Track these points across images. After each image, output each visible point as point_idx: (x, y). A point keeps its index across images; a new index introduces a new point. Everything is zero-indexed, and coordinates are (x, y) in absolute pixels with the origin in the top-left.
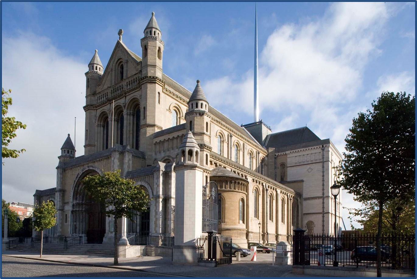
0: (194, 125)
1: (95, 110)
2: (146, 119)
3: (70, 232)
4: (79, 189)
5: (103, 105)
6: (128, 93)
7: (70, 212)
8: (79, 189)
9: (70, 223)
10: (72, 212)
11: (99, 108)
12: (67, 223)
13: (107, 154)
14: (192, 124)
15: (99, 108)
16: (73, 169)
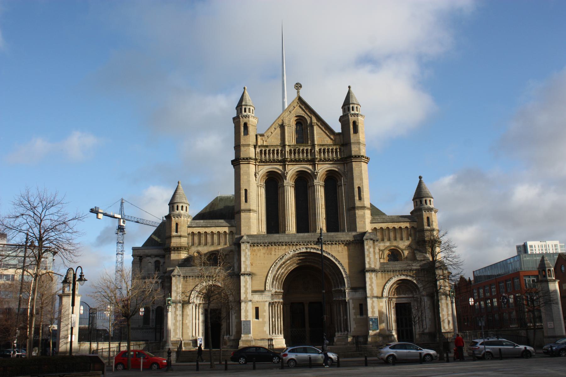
0: (432, 222)
1: (257, 166)
2: (364, 201)
3: (268, 332)
4: (278, 274)
5: (273, 163)
6: (322, 162)
7: (267, 304)
8: (278, 274)
9: (267, 319)
10: (271, 304)
11: (263, 164)
12: (260, 319)
13: (348, 239)
14: (430, 221)
15: (263, 164)
16: (270, 247)
